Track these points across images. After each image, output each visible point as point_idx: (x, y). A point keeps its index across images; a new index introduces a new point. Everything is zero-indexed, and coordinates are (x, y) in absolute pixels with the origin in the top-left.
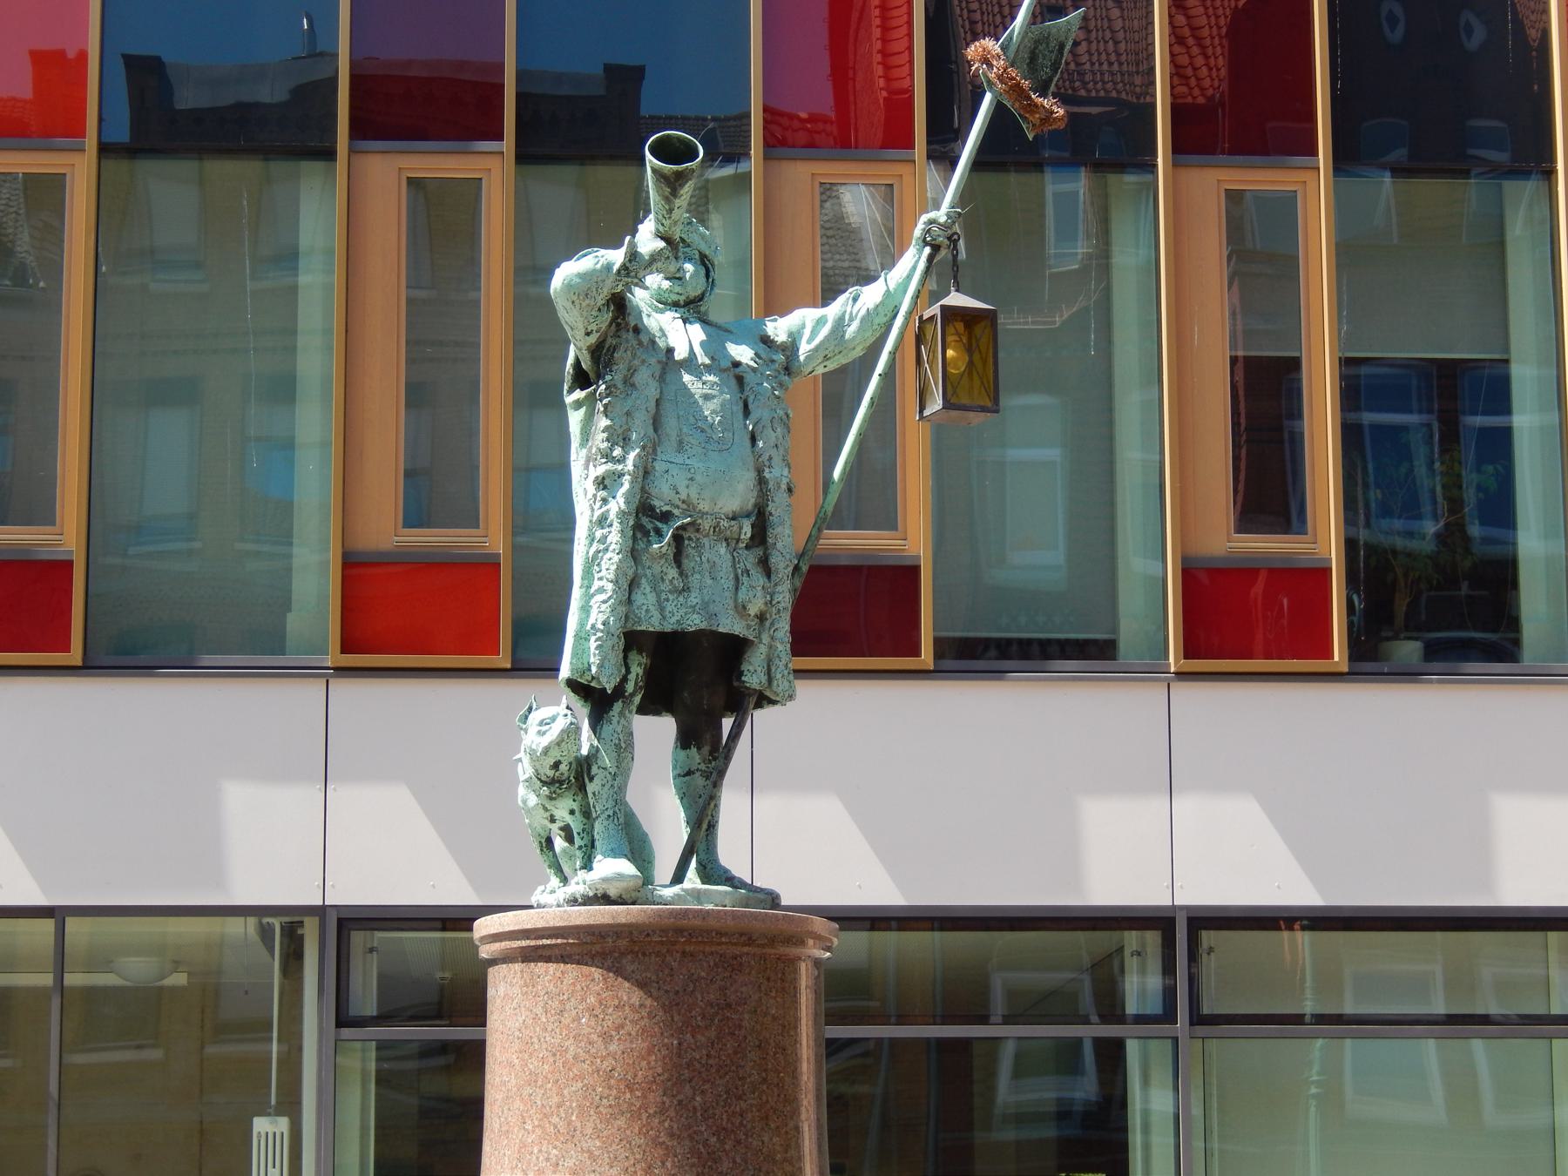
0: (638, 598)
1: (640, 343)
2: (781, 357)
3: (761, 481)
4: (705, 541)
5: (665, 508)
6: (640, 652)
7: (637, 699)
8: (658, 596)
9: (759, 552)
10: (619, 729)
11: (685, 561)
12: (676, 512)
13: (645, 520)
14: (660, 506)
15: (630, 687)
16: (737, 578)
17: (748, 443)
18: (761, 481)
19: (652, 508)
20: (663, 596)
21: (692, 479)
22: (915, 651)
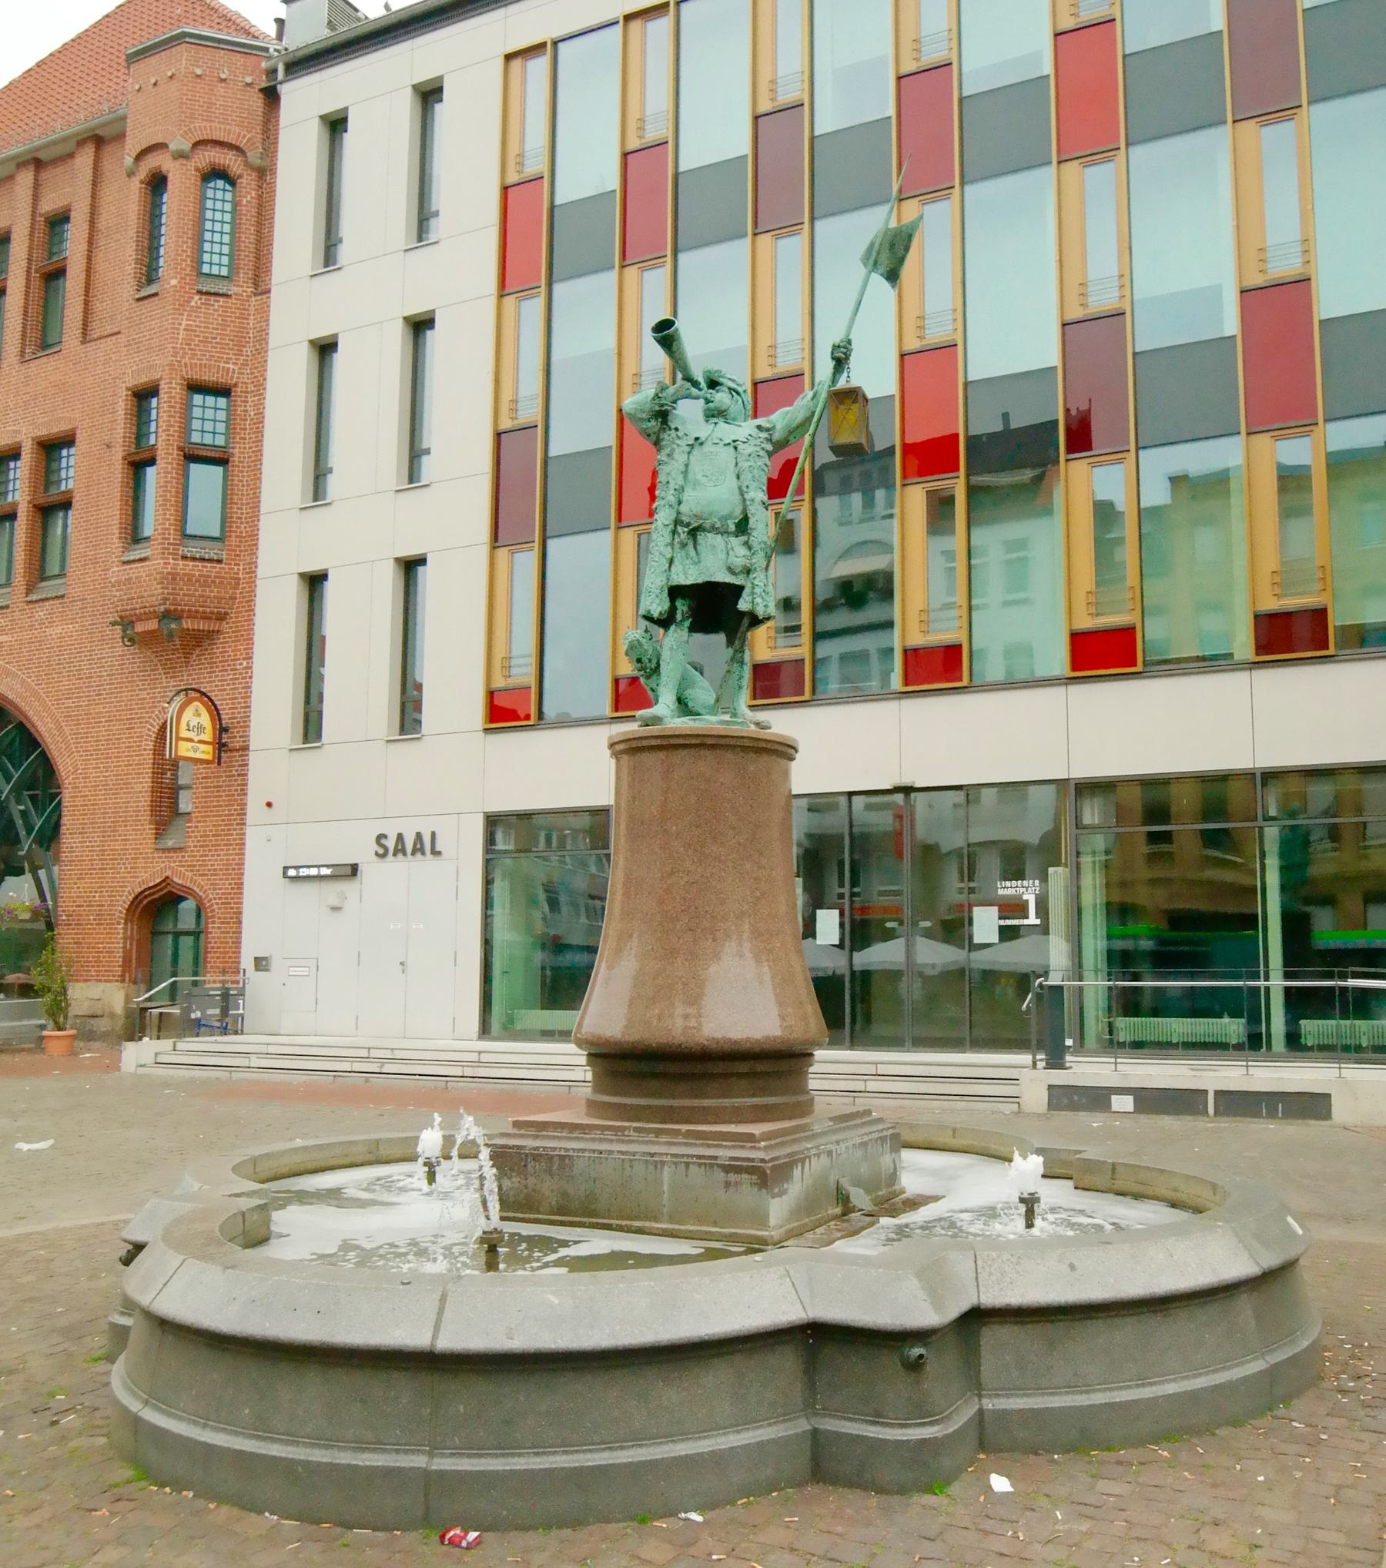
0: (673, 568)
2: (764, 435)
3: (744, 500)
6: (683, 598)
7: (687, 623)
9: (744, 538)
13: (680, 529)
14: (685, 519)
15: (679, 617)
22: (1325, 645)
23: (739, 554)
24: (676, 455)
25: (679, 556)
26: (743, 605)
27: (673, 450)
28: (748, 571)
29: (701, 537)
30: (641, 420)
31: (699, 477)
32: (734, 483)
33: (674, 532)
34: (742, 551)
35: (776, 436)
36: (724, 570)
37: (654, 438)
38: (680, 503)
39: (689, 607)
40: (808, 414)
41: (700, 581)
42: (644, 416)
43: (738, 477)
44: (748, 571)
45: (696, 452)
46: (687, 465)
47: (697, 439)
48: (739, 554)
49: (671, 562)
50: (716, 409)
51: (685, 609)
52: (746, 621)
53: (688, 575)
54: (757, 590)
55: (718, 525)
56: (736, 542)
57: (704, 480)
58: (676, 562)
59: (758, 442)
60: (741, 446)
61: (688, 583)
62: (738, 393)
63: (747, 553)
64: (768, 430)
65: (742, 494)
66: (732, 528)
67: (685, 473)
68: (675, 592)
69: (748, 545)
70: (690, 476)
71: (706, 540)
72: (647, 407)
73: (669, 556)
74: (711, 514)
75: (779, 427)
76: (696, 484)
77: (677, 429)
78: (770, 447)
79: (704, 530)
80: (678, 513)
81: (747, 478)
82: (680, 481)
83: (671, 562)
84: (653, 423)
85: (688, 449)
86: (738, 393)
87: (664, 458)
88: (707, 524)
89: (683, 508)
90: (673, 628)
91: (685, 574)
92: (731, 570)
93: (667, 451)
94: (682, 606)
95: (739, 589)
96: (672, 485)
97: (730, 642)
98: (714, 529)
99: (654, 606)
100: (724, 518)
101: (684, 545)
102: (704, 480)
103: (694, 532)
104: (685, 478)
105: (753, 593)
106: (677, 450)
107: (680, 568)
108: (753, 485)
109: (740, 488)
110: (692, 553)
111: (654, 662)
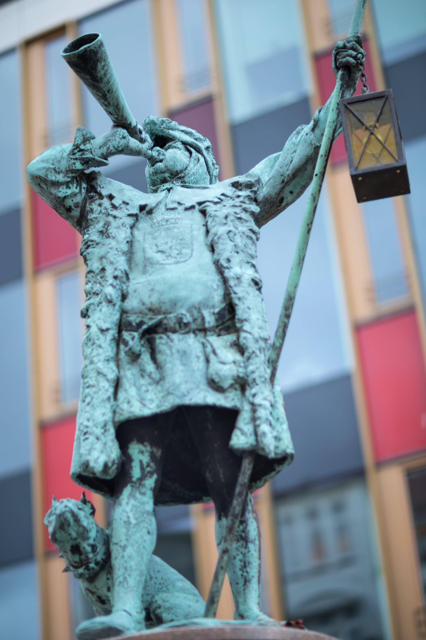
0: (121, 395)
1: (114, 207)
3: (225, 281)
4: (175, 337)
5: (138, 321)
6: (141, 441)
7: (150, 482)
8: (139, 389)
10: (128, 508)
11: (160, 357)
12: (145, 320)
13: (126, 335)
14: (134, 319)
15: (136, 473)
16: (207, 361)
17: (207, 254)
18: (225, 281)
19: (130, 324)
20: (144, 388)
21: (152, 290)
23: (227, 362)
24: (112, 230)
25: (129, 373)
26: (240, 440)
27: (107, 224)
28: (242, 384)
29: (161, 341)
30: (56, 184)
31: (151, 253)
32: (207, 257)
33: (119, 341)
34: (231, 355)
35: (263, 192)
36: (204, 386)
37: (76, 213)
38: (124, 297)
39: (153, 456)
40: (309, 151)
41: (166, 406)
42: (60, 178)
43: (212, 249)
44: (242, 384)
45: (144, 225)
46: (130, 243)
47: (142, 208)
48: (227, 362)
49: (117, 385)
50: (168, 170)
51: (146, 459)
52: (247, 467)
53: (144, 401)
54: (262, 413)
55: (188, 318)
56: (220, 343)
57: (159, 257)
58: (126, 384)
59: (237, 202)
60: (211, 209)
61: (147, 412)
62: (199, 151)
63: (238, 357)
64: (249, 186)
65: (220, 269)
66: (210, 320)
67: (130, 255)
68: (127, 431)
69: (241, 349)
70: (138, 256)
71: (173, 346)
72: (64, 165)
73: (112, 376)
74: (174, 303)
75: (265, 178)
76: (148, 264)
77: (111, 197)
78: (255, 209)
79: (166, 330)
80: (123, 312)
81: (225, 249)
82: (122, 263)
83: (117, 385)
84: (74, 189)
85: (130, 221)
86: (199, 151)
87: (95, 237)
88: (171, 320)
89: (132, 303)
90: (127, 490)
91: (142, 401)
92: (214, 385)
93: (100, 226)
94: (141, 454)
95: (227, 418)
96: (109, 272)
97: (223, 510)
98: (182, 326)
99: (95, 454)
100: (198, 308)
101: (135, 357)
102: (159, 257)
103: (150, 334)
104: (130, 261)
105: (254, 419)
106: (114, 223)
107: (133, 391)
108: (236, 259)
109: (217, 264)
110: (150, 367)
111: (101, 549)
